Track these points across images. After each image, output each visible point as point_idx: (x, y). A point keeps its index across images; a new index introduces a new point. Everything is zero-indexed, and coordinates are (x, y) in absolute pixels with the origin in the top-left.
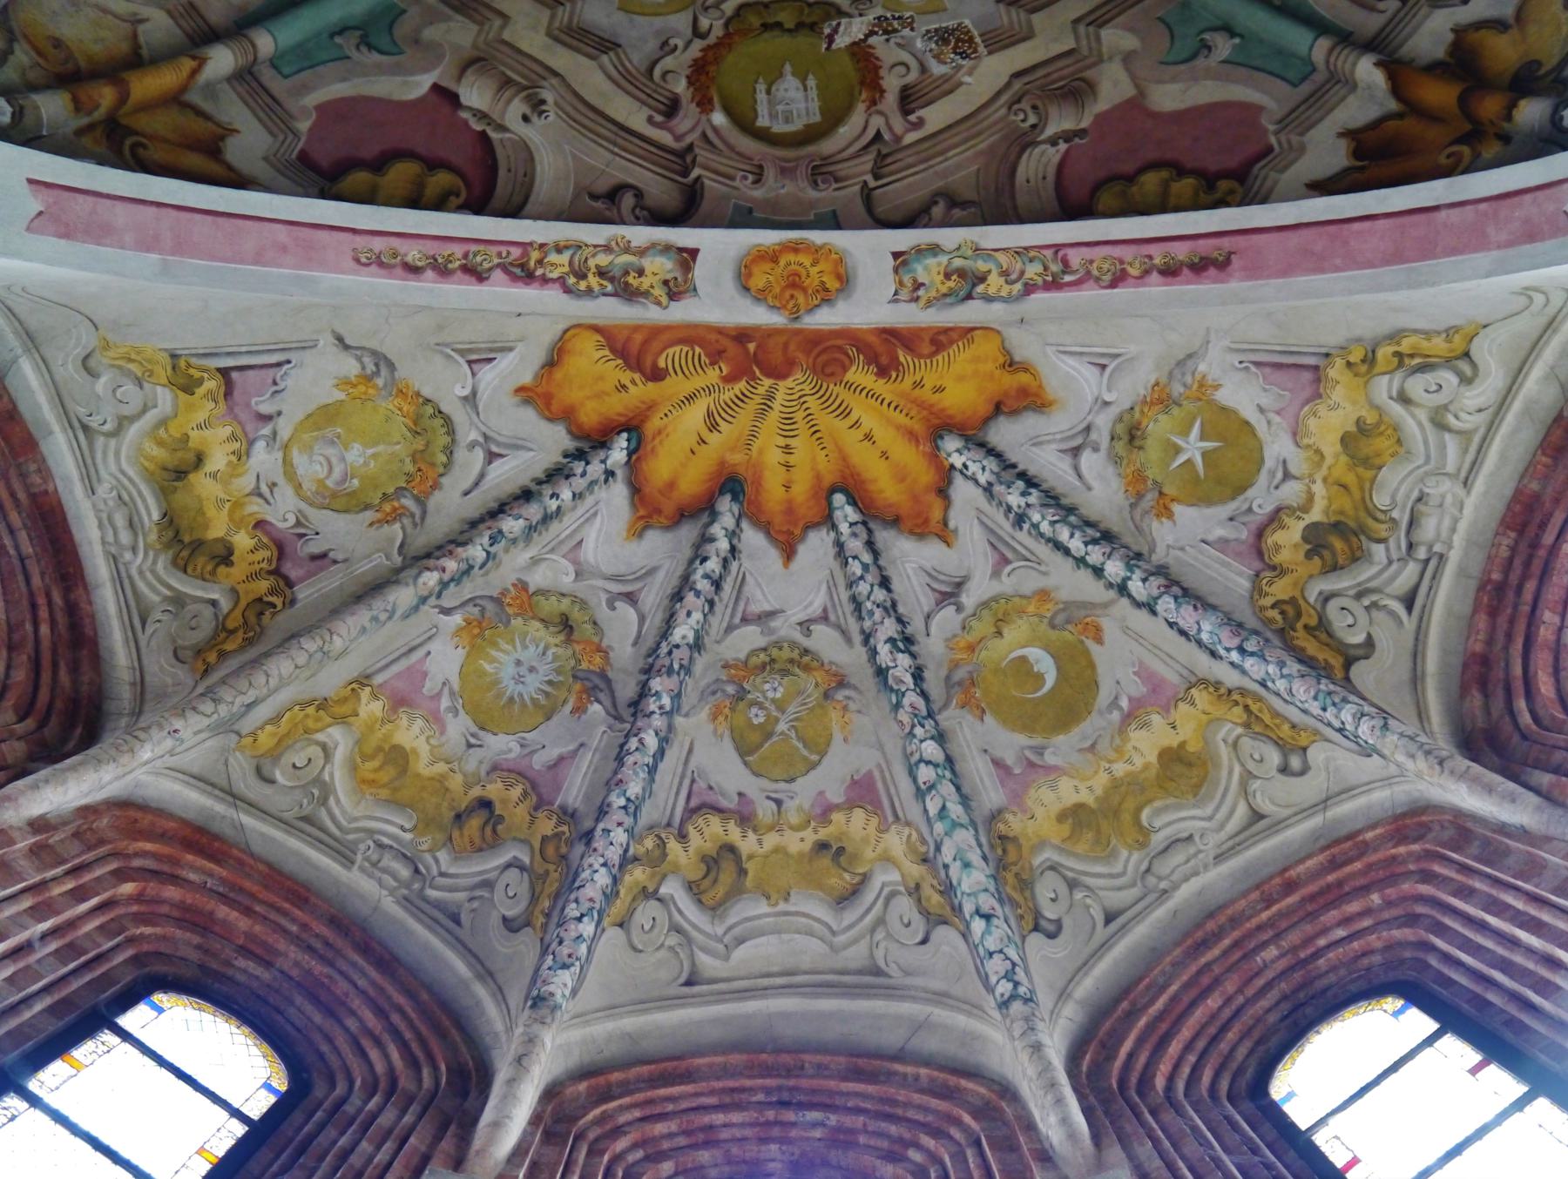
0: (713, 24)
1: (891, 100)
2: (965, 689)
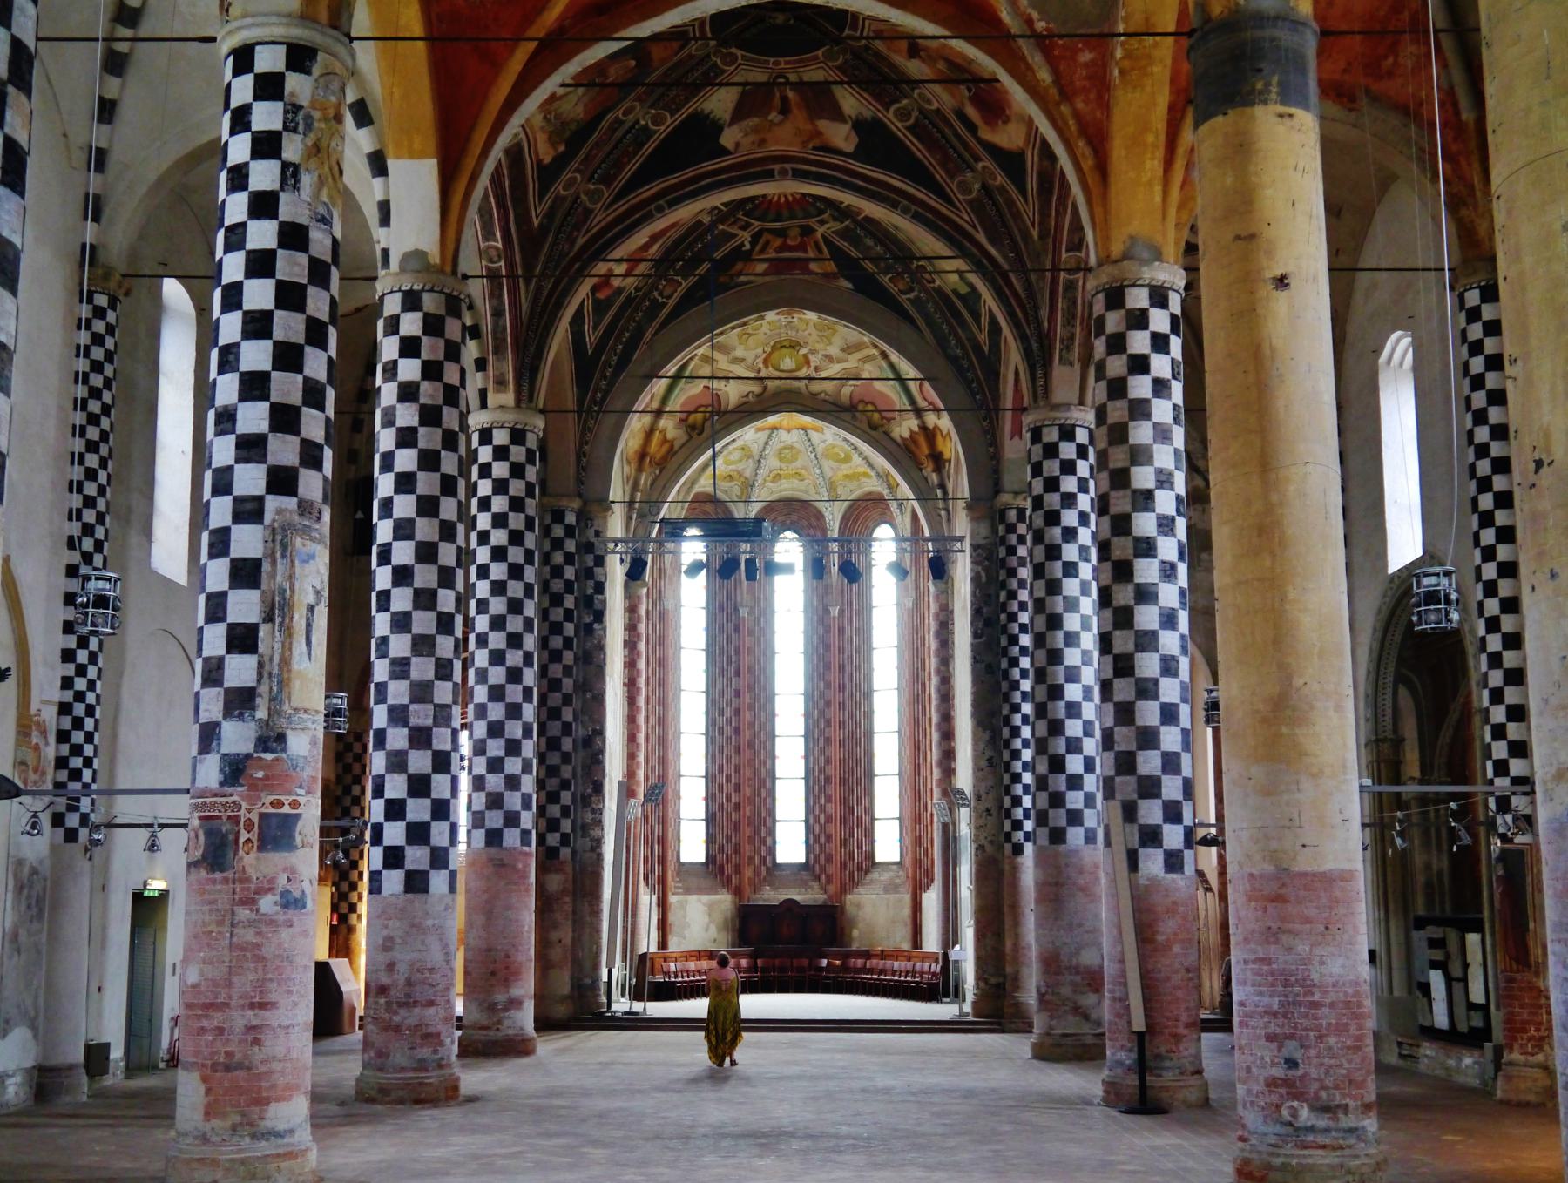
0: (768, 349)
1: (812, 368)
2: (826, 455)
